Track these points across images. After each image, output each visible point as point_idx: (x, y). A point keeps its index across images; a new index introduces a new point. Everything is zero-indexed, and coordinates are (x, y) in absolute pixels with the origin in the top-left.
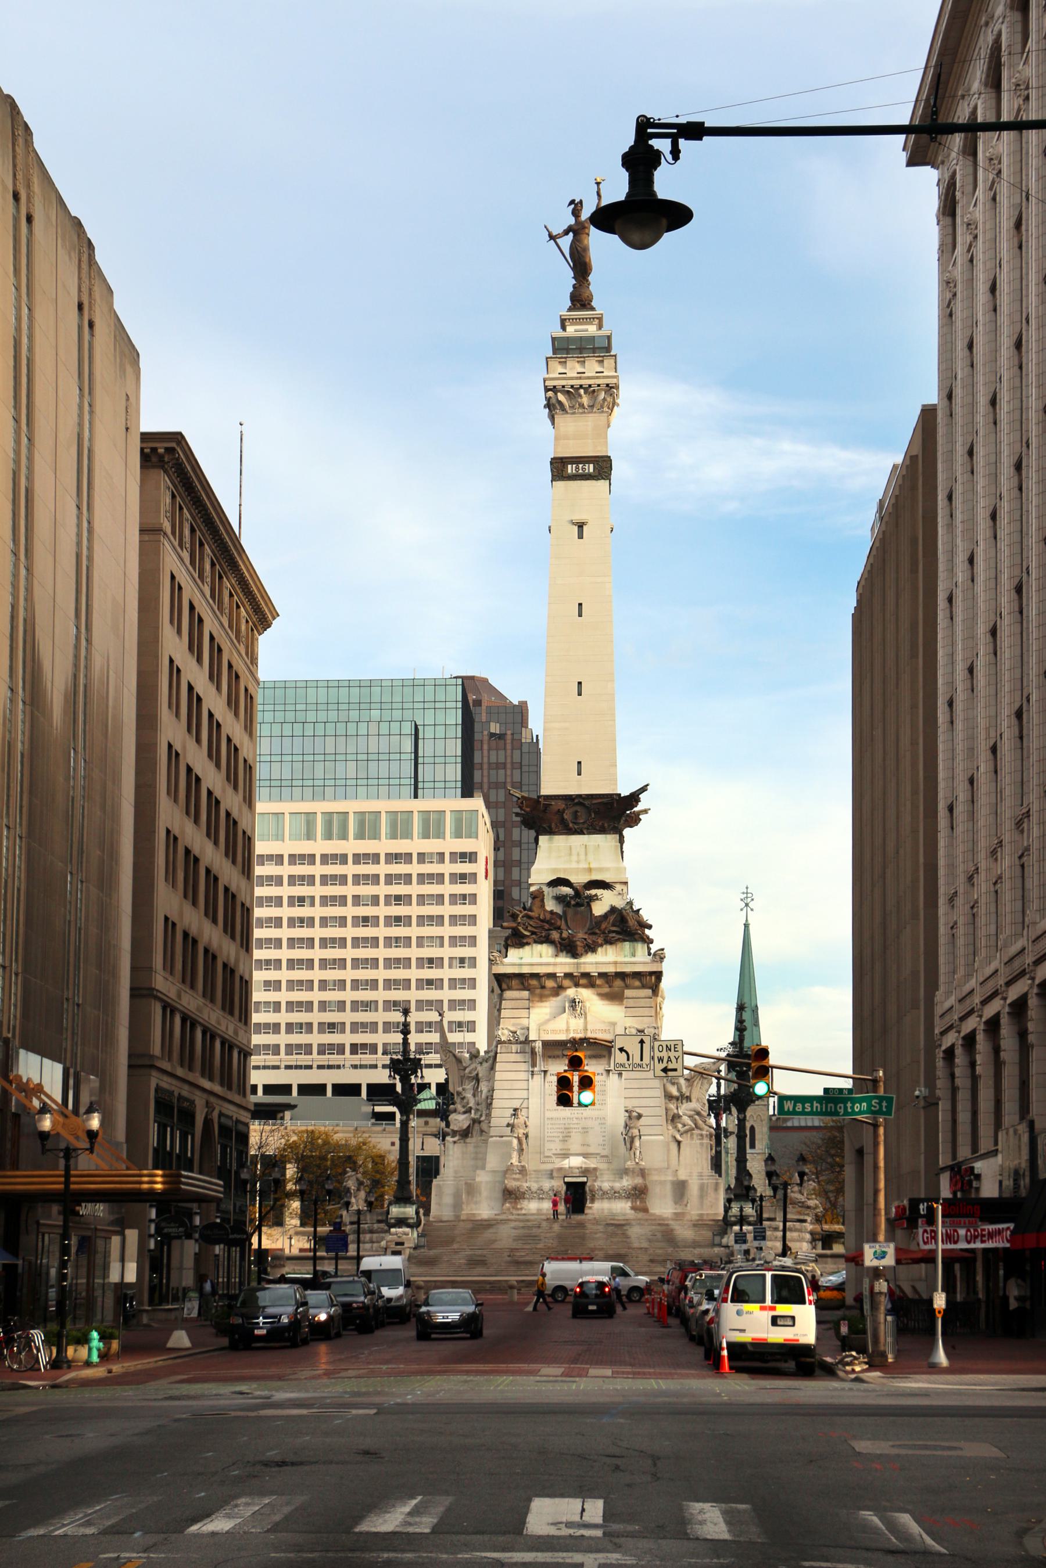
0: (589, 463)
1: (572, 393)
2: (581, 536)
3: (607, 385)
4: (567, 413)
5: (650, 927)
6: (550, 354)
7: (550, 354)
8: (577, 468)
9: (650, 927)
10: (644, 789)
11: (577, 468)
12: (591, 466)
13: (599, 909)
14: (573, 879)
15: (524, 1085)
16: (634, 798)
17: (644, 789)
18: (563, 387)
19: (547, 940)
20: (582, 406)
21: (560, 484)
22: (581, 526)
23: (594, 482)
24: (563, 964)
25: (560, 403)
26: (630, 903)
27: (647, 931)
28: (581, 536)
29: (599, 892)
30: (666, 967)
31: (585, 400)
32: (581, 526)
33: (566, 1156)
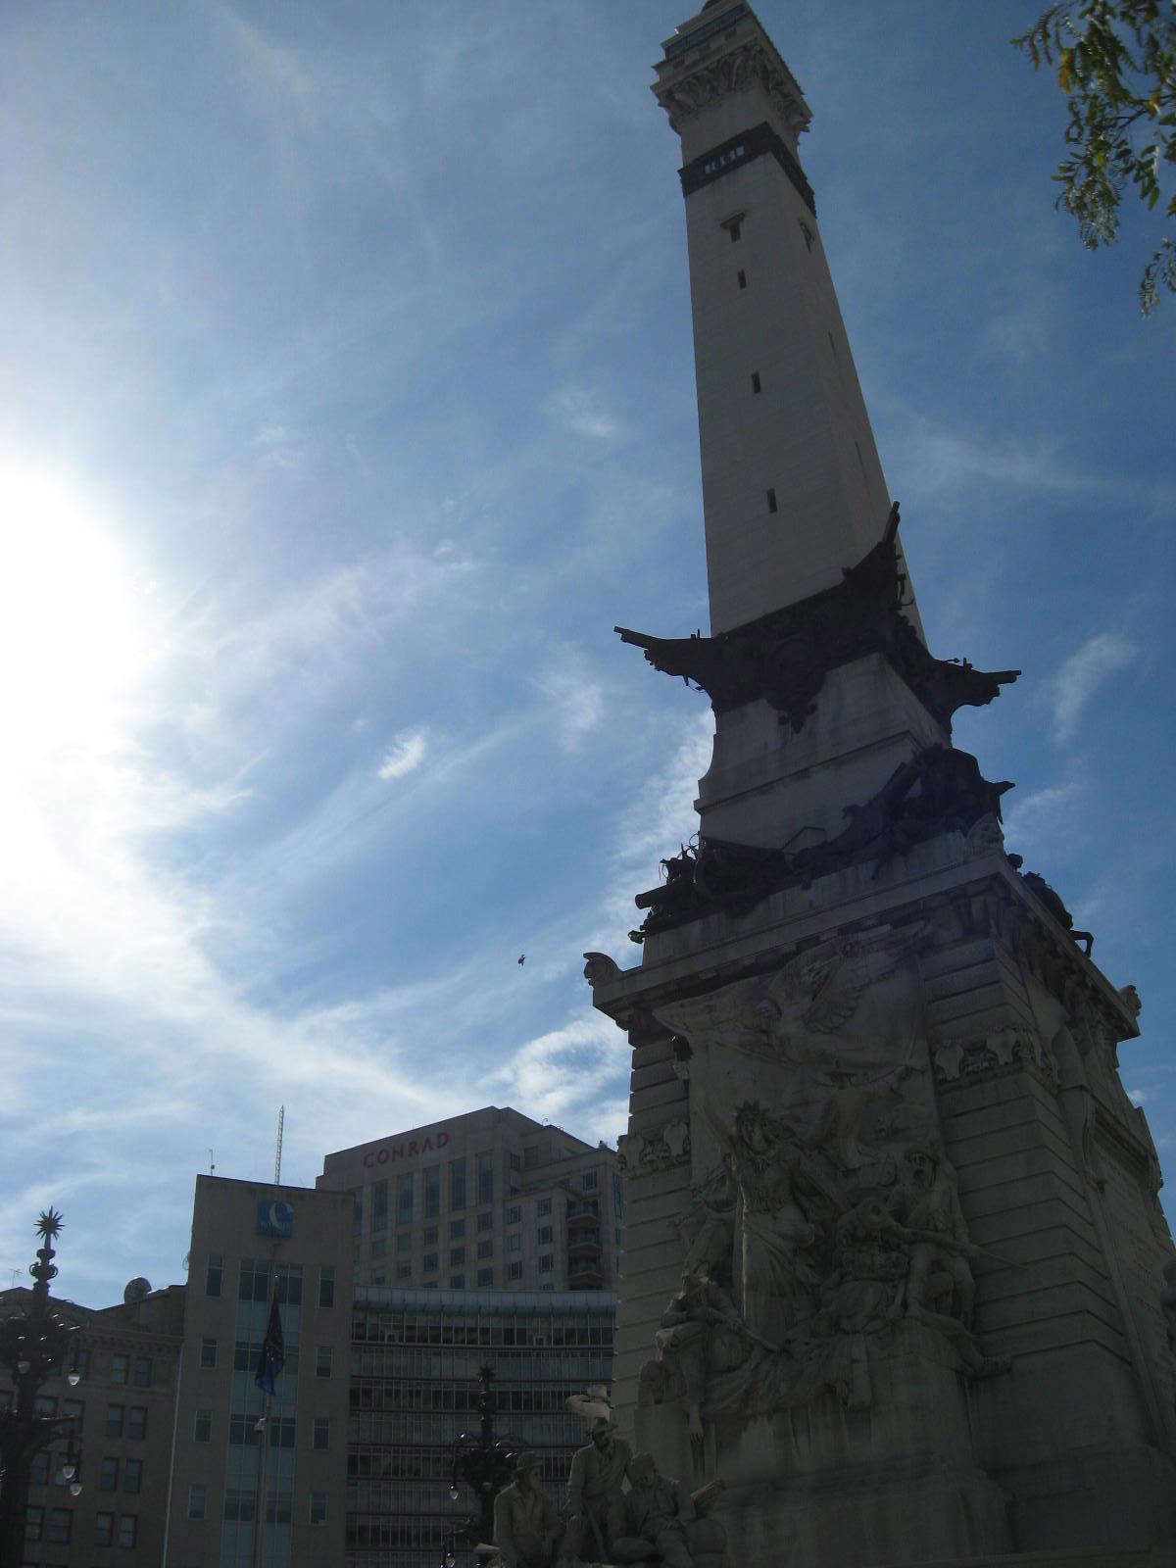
18: (681, 83)
32: (733, 226)
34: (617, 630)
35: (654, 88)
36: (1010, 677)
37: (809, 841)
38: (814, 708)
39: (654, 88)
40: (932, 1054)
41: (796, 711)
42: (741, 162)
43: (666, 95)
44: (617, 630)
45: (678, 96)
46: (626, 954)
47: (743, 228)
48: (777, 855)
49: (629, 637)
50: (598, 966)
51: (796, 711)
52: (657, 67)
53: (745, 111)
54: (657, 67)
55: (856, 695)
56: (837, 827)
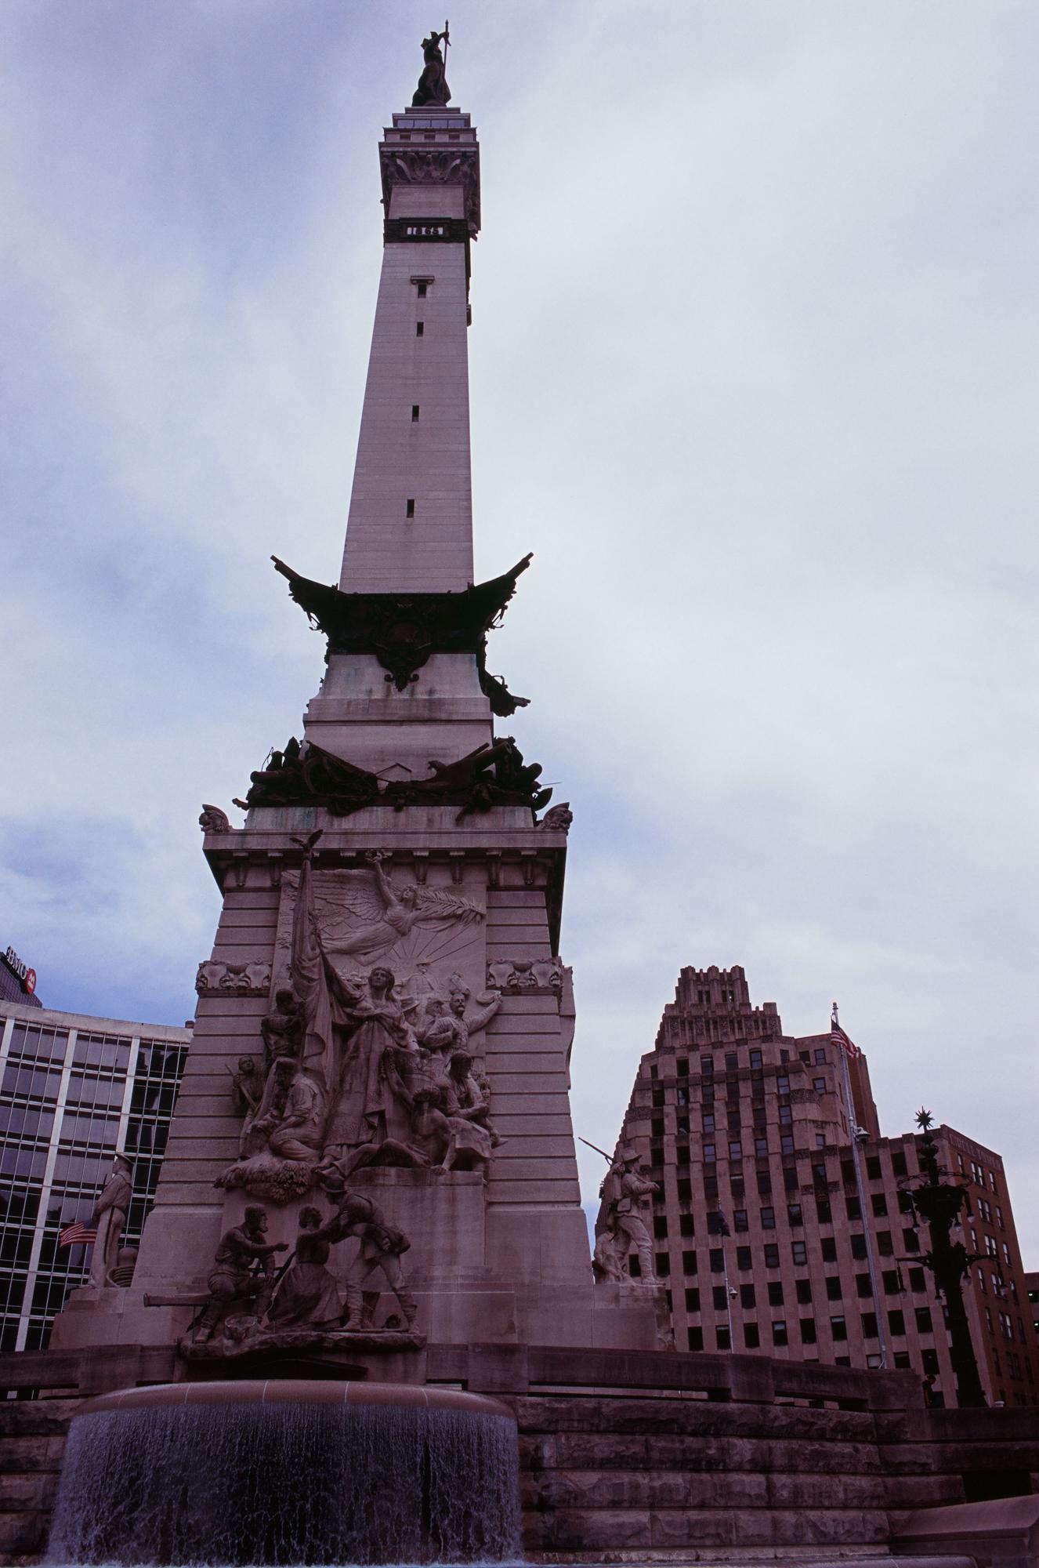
0: (436, 227)
1: (417, 160)
3: (464, 153)
4: (409, 182)
6: (391, 126)
7: (391, 126)
8: (419, 231)
10: (524, 564)
11: (419, 231)
12: (441, 231)
16: (501, 590)
17: (524, 564)
18: (405, 153)
20: (428, 175)
21: (395, 245)
23: (444, 245)
25: (399, 168)
31: (436, 174)
32: (422, 285)
34: (273, 558)
35: (381, 145)
37: (395, 776)
38: (416, 678)
39: (381, 145)
40: (488, 965)
41: (402, 673)
42: (436, 239)
44: (273, 558)
45: (399, 161)
46: (237, 819)
47: (429, 289)
48: (372, 779)
49: (281, 567)
50: (212, 819)
51: (402, 673)
52: (387, 131)
53: (445, 204)
54: (387, 131)
55: (446, 678)
56: (421, 772)
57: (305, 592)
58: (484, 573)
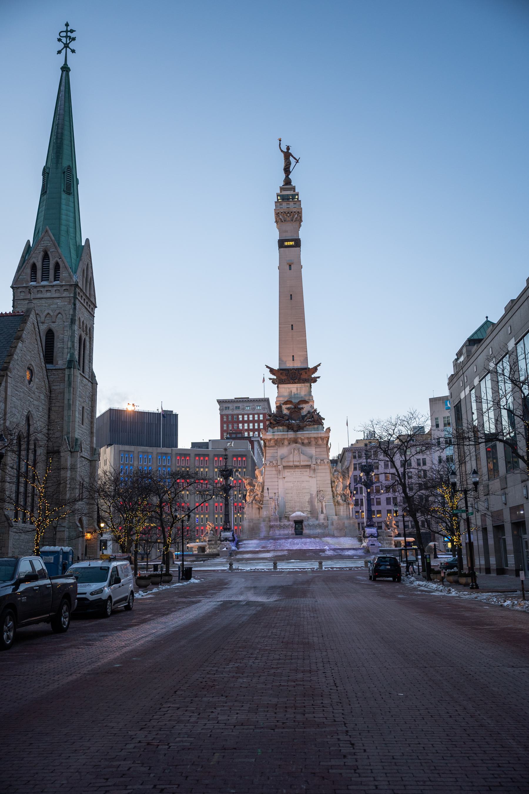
2: (290, 269)
5: (324, 419)
9: (324, 419)
10: (319, 365)
13: (304, 412)
14: (293, 401)
15: (276, 483)
17: (319, 365)
19: (282, 425)
21: (282, 249)
22: (290, 266)
24: (291, 435)
26: (316, 410)
27: (323, 421)
28: (290, 269)
29: (304, 405)
30: (331, 434)
32: (290, 266)
33: (294, 512)
36: (319, 377)
43: (277, 214)
49: (267, 367)
57: (272, 371)
58: (311, 366)
